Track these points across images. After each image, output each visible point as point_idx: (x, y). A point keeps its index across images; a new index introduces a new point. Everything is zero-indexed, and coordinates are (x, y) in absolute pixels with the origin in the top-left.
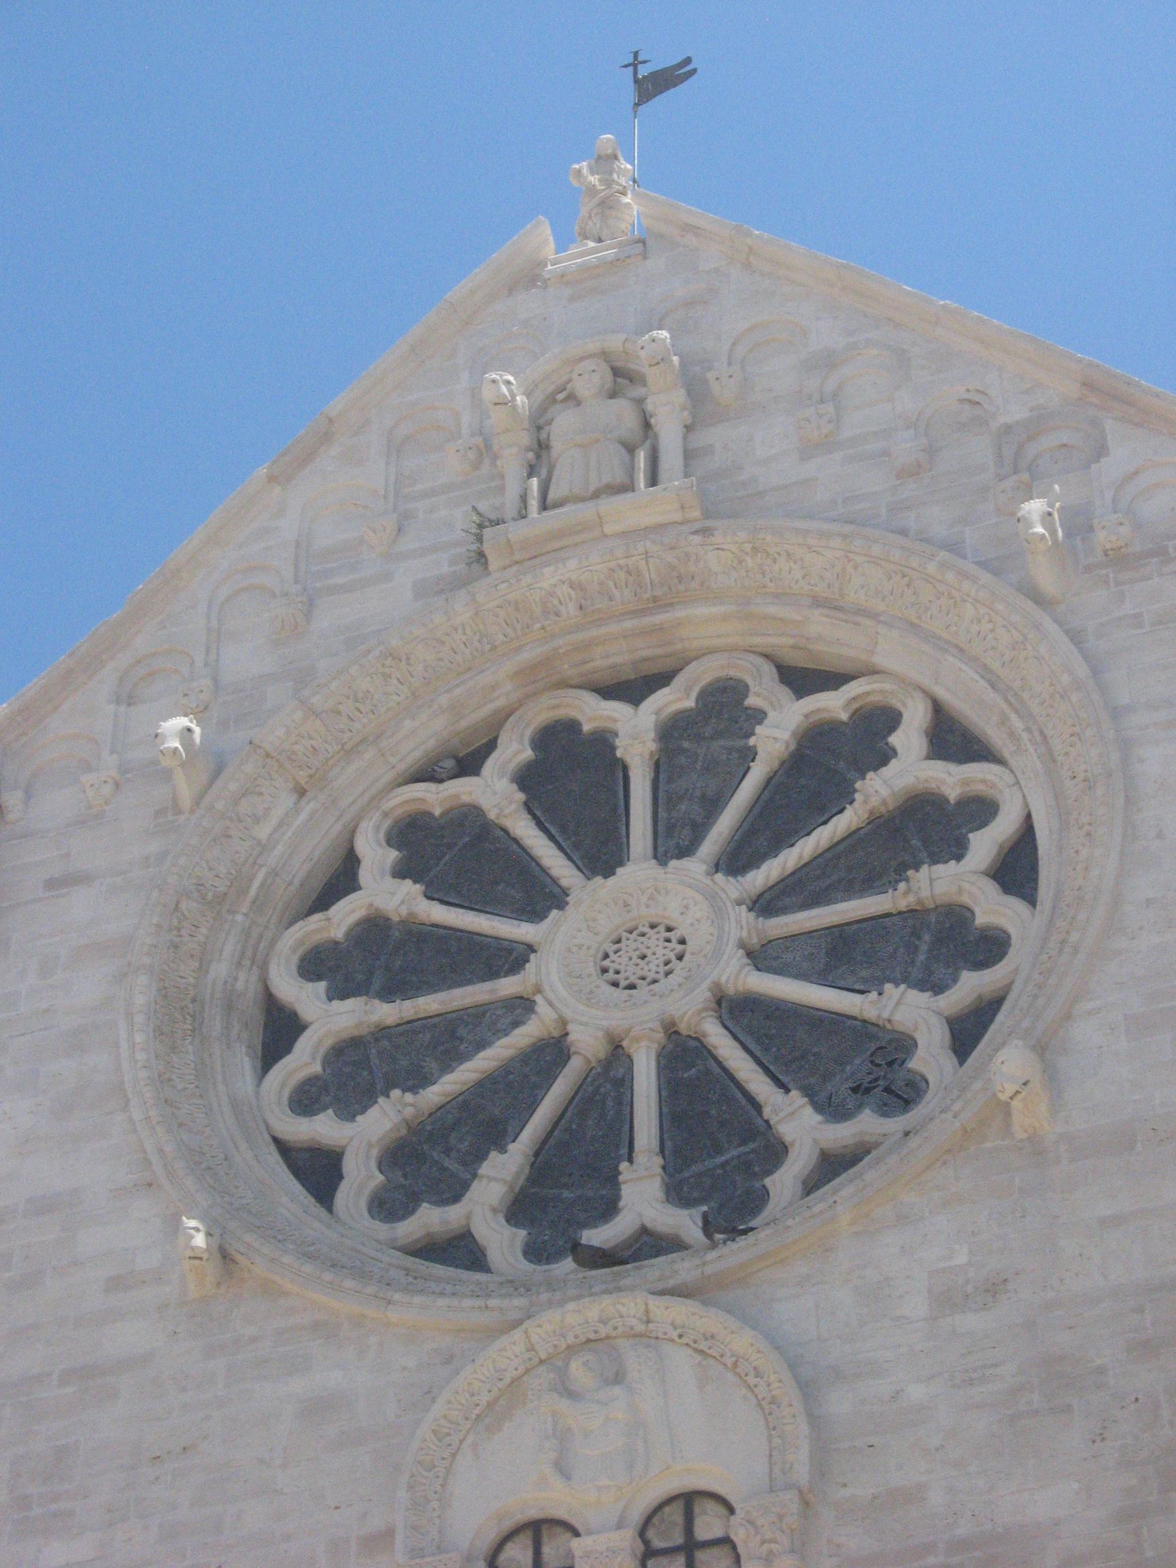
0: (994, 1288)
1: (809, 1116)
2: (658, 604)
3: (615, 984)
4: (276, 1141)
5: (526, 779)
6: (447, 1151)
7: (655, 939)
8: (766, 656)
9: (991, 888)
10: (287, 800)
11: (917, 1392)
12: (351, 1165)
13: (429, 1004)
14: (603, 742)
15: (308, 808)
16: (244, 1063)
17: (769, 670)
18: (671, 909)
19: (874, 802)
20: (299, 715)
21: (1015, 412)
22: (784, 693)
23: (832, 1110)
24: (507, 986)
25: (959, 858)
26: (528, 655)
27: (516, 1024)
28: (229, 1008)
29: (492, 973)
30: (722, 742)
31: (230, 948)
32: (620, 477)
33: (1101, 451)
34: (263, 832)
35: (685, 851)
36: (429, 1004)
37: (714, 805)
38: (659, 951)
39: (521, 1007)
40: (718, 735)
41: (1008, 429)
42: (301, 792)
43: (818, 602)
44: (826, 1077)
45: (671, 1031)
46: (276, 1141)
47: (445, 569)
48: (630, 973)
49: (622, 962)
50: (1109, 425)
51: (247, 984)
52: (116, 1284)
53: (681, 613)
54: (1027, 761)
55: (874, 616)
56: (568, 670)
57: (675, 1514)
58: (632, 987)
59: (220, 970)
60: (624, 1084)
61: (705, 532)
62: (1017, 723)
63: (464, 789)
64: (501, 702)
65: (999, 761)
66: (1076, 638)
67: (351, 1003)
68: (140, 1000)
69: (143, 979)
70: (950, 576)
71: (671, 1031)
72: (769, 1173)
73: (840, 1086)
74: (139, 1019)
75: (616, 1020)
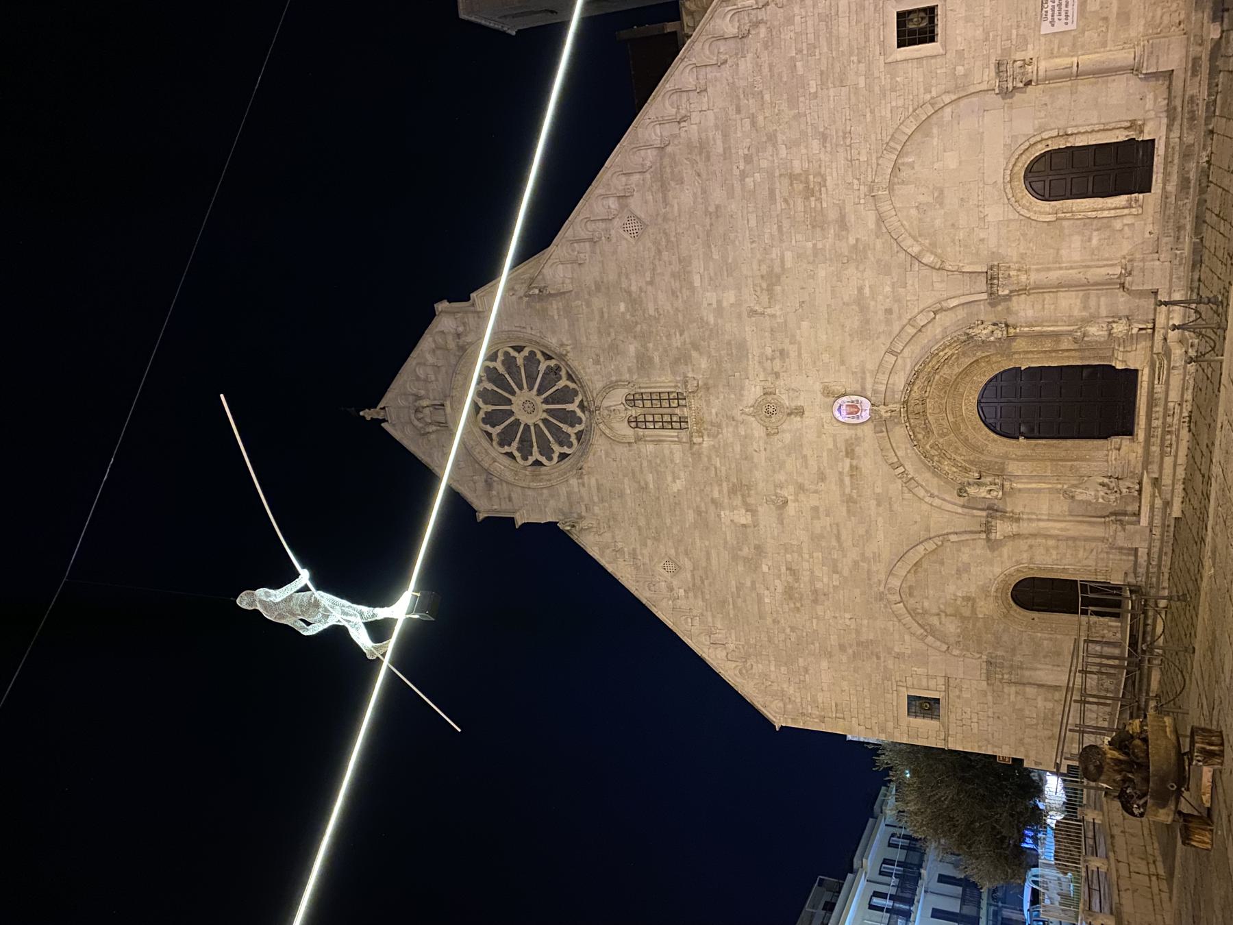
0: (597, 355)
7: (526, 406)
9: (522, 353)
11: (613, 367)
12: (562, 452)
13: (534, 440)
16: (543, 468)
18: (521, 403)
23: (560, 378)
27: (539, 426)
35: (510, 400)
36: (534, 440)
38: (528, 404)
45: (543, 403)
48: (532, 409)
49: (529, 411)
57: (628, 402)
63: (494, 436)
64: (479, 430)
71: (543, 403)
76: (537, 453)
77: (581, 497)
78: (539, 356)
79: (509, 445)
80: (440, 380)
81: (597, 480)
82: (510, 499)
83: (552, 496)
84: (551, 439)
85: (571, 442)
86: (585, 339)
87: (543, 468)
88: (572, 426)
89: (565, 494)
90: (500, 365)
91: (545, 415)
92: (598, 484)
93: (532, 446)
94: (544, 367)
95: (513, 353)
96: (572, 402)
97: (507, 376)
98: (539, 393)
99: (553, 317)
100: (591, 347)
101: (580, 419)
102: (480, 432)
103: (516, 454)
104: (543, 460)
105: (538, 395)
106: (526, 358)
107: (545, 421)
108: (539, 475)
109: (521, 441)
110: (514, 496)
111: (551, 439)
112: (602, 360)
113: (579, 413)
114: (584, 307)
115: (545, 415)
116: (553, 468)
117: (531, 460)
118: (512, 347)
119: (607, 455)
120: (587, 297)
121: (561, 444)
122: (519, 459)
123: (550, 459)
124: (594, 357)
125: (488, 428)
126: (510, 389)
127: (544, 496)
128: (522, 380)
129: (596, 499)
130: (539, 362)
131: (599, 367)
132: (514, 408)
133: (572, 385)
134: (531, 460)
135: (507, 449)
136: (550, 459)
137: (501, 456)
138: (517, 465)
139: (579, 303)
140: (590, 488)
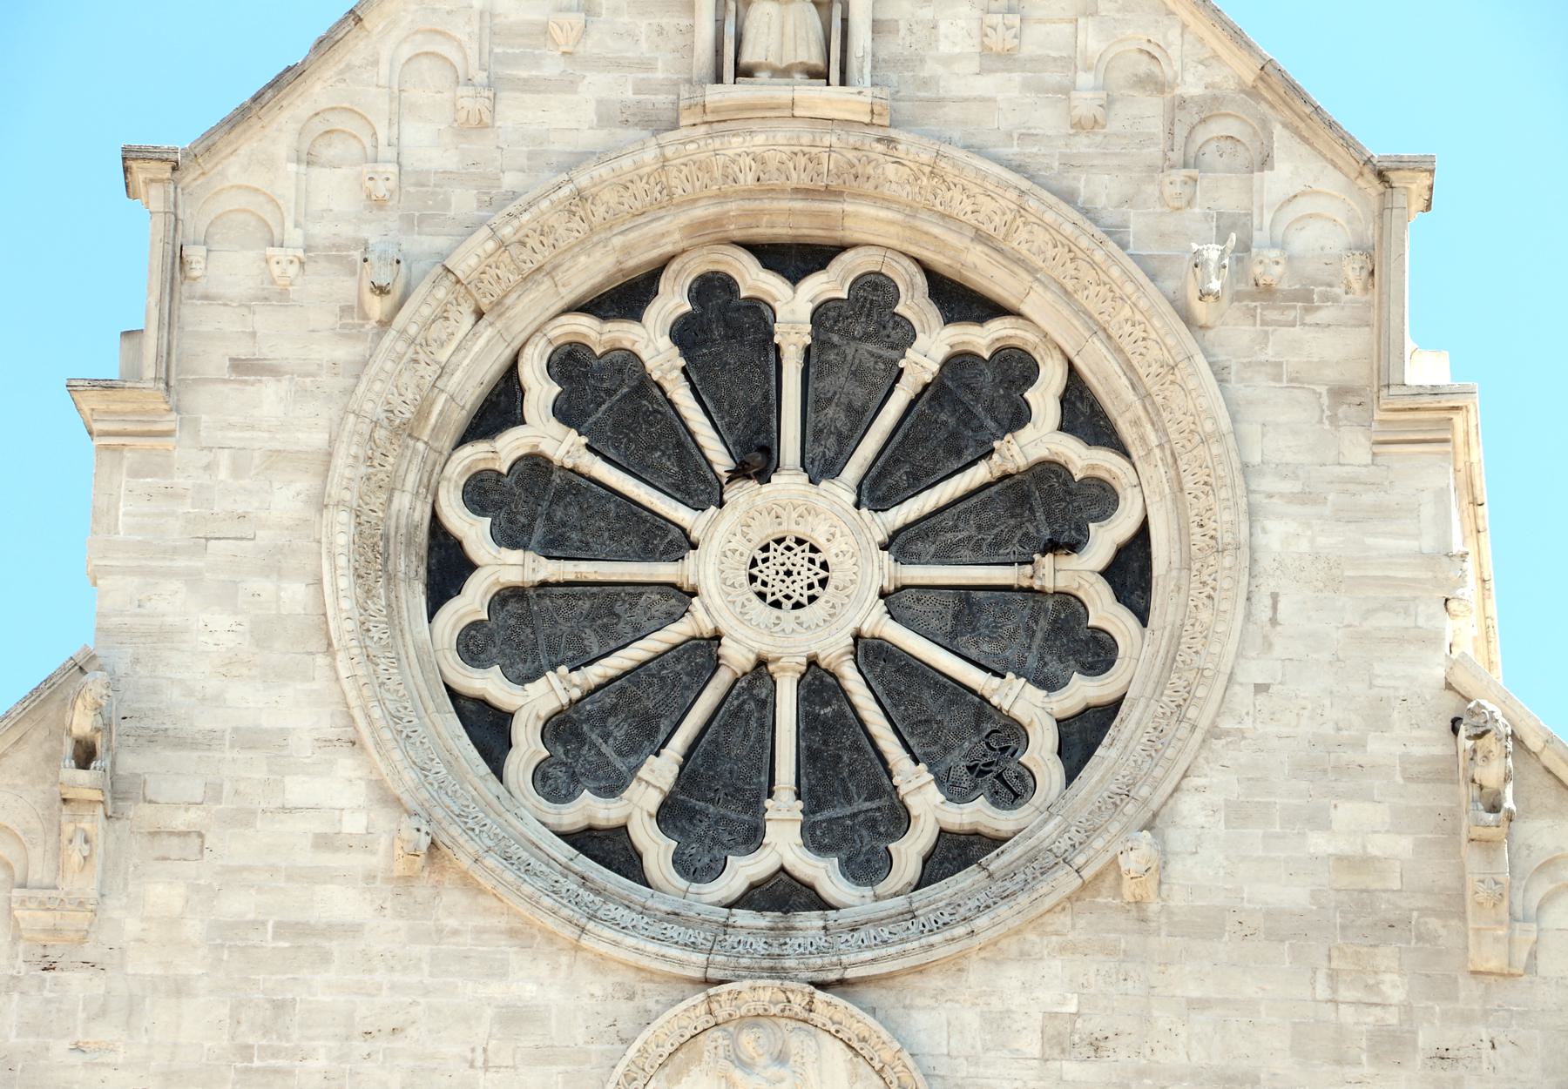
1: (934, 795)
2: (830, 193)
3: (762, 596)
4: (453, 694)
5: (684, 334)
6: (606, 736)
7: (800, 557)
8: (917, 261)
10: (471, 319)
14: (759, 314)
15: (486, 332)
17: (921, 281)
19: (1010, 468)
20: (490, 246)
21: (1191, 86)
22: (933, 313)
23: (954, 791)
24: (663, 571)
25: (1074, 547)
26: (700, 212)
27: (673, 618)
28: (409, 543)
29: (647, 554)
30: (870, 347)
31: (412, 479)
32: (814, 58)
33: (1265, 162)
34: (443, 356)
37: (861, 420)
38: (808, 574)
39: (705, 651)
40: (866, 337)
41: (1182, 103)
42: (480, 315)
43: (980, 237)
44: (947, 749)
45: (812, 662)
46: (453, 694)
47: (629, 95)
48: (777, 589)
49: (767, 572)
50: (1278, 130)
51: (422, 515)
52: (325, 842)
53: (849, 207)
54: (1155, 474)
55: (1032, 271)
56: (738, 235)
58: (777, 604)
59: (402, 501)
60: (767, 705)
61: (890, 141)
62: (1153, 438)
63: (621, 333)
64: (667, 248)
65: (1124, 451)
66: (1220, 373)
67: (516, 556)
68: (342, 540)
69: (344, 516)
70: (1115, 272)
71: (812, 662)
72: (894, 837)
73: (957, 761)
74: (342, 561)
75: (767, 647)
76: (513, 577)
77: (243, 818)
78: (1082, 691)
79: (566, 413)
80: (986, 85)
81: (352, 930)
82: (243, 367)
83: (263, 634)
84: (596, 673)
85: (568, 797)
86: (1194, 991)
87: (421, 602)
88: (670, 815)
89: (269, 721)
90: (1037, 453)
91: (737, 655)
92: (332, 930)
93: (554, 548)
94: (1020, 712)
95: (1105, 539)
96: (816, 839)
97: (979, 474)
98: (868, 650)
99: (1317, 820)
100: (1146, 1019)
101: (713, 871)
102: (653, 254)
103: (507, 448)
104: (471, 602)
105: (857, 637)
106: (1070, 606)
107: (705, 651)
108: (391, 579)
109: (578, 485)
110: (269, 397)
111: (596, 673)
112: (1071, 1069)
113: (743, 871)
114: (1371, 1017)
115: (737, 655)
116: (426, 659)
117: (472, 531)
118: (1143, 533)
119: (514, 1017)
120: (1426, 1038)
121: (560, 728)
122: (475, 454)
123: (473, 646)
124: (1095, 1024)
125: (672, 301)
126: (900, 475)
127: (265, 586)
128: (944, 557)
129: (238, 905)
130: (1048, 684)
131: (1031, 1045)
132: (789, 483)
133: (909, 852)
134: (472, 531)
135: (540, 390)
136: (473, 646)
137: (503, 355)
138: (447, 442)
139: (1394, 988)
140: (312, 877)
